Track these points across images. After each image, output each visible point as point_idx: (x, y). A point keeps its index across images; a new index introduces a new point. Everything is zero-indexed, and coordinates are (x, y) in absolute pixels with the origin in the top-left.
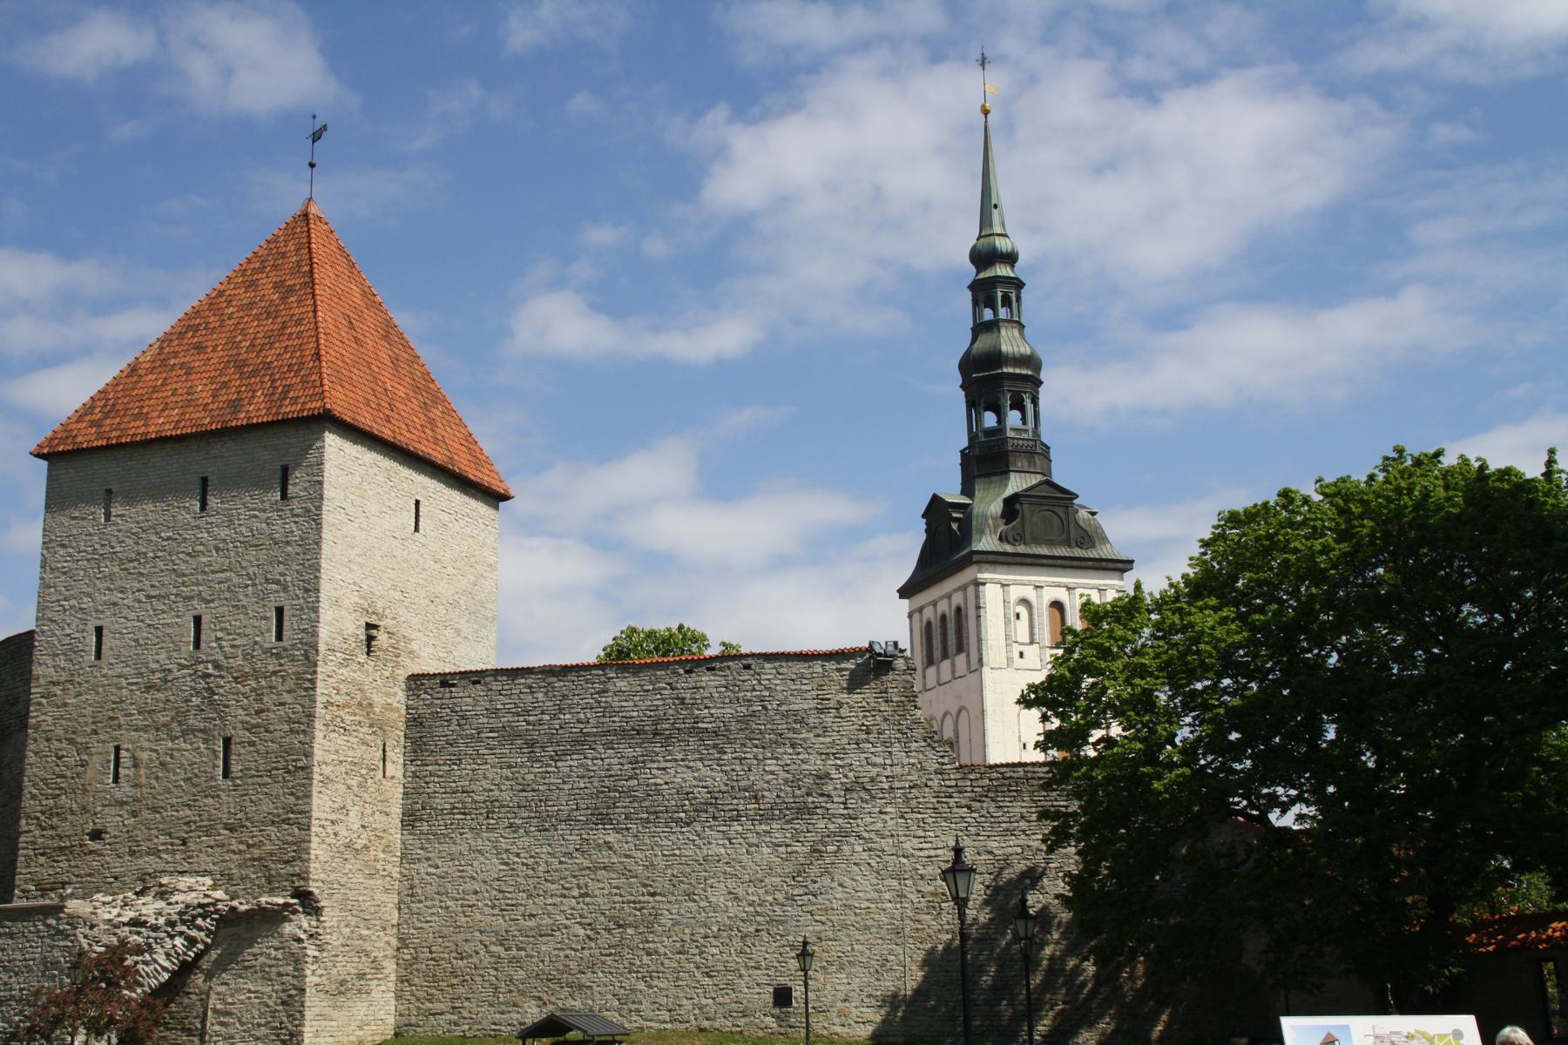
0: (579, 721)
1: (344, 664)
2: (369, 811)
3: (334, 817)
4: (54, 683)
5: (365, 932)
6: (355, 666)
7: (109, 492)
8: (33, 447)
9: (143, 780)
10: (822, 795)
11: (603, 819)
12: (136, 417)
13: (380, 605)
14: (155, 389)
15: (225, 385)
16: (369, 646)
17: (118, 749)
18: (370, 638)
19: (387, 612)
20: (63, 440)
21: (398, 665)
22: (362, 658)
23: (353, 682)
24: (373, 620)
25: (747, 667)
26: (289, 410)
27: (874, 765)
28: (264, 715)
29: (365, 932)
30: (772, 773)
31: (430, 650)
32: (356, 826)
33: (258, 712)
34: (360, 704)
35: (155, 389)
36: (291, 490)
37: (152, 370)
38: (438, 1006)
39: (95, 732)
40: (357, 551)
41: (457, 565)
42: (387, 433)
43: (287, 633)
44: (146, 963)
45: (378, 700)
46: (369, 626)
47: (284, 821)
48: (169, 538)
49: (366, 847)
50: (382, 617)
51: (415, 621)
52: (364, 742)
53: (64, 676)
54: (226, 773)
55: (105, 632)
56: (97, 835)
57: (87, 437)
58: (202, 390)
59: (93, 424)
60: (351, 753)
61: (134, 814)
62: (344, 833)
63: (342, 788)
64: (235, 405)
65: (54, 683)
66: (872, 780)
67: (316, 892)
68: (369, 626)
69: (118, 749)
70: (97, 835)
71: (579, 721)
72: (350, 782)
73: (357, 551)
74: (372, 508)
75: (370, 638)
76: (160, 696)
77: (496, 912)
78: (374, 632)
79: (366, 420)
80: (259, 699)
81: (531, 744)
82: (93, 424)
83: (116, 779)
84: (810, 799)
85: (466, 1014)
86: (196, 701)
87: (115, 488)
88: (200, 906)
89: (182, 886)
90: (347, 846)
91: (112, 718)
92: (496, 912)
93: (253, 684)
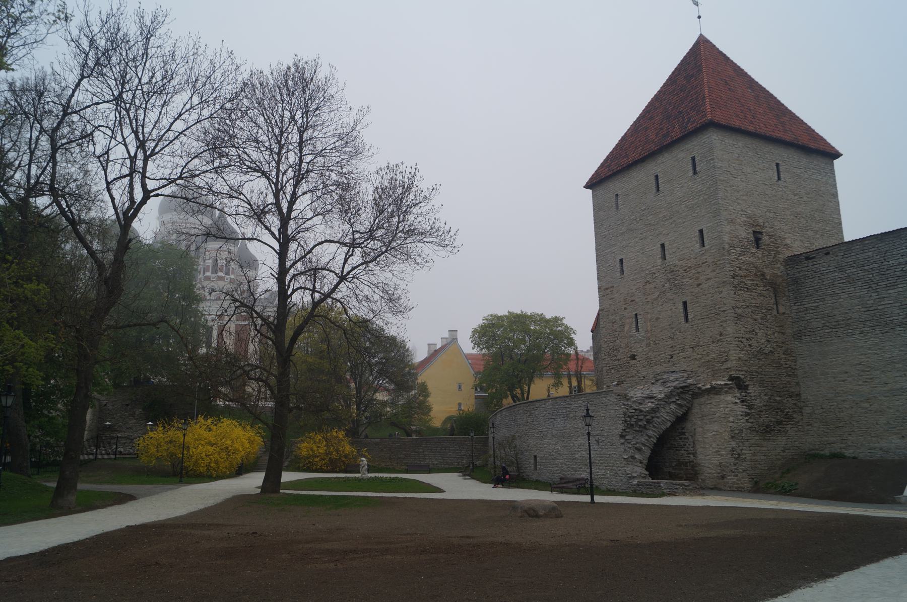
1: (743, 253)
3: (747, 336)
4: (607, 289)
7: (617, 195)
12: (624, 157)
15: (662, 129)
17: (636, 315)
19: (766, 224)
22: (754, 250)
24: (758, 229)
32: (763, 341)
33: (699, 285)
34: (756, 275)
39: (625, 309)
40: (741, 193)
42: (751, 128)
43: (706, 242)
44: (658, 417)
53: (610, 285)
54: (687, 320)
56: (633, 357)
60: (753, 301)
62: (755, 344)
65: (607, 289)
69: (636, 315)
70: (633, 357)
72: (755, 317)
73: (741, 193)
76: (652, 286)
78: (760, 236)
79: (736, 123)
80: (697, 279)
83: (637, 330)
86: (667, 285)
88: (681, 387)
90: (758, 352)
93: (693, 271)
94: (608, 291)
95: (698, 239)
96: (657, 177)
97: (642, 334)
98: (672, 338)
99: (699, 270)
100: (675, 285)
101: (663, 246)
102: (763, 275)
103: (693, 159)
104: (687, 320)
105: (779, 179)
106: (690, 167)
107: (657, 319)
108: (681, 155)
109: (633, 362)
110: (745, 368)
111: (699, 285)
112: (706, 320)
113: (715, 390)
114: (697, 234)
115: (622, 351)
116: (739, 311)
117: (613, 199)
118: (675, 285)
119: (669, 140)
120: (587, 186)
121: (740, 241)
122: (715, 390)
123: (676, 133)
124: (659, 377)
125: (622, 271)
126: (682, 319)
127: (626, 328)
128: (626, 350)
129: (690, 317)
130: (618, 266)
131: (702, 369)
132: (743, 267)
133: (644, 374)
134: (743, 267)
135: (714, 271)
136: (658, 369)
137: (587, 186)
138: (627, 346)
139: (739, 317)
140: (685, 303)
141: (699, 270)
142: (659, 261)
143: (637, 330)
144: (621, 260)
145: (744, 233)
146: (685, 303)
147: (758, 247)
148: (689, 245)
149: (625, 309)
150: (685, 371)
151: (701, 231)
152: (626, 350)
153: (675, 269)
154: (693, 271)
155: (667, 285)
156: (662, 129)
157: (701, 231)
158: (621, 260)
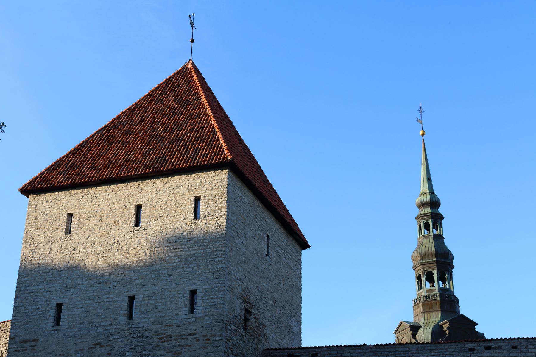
6: (240, 337)
12: (93, 167)
13: (251, 298)
15: (152, 149)
16: (245, 326)
18: (246, 320)
21: (259, 342)
22: (243, 332)
31: (273, 335)
43: (198, 308)
55: (64, 307)
68: (247, 311)
73: (241, 258)
74: (249, 233)
75: (246, 320)
87: (75, 213)
93: (174, 342)
94: (26, 345)
95: (187, 301)
96: (139, 208)
99: (183, 342)
103: (197, 200)
114: (188, 294)
117: (64, 218)
125: (58, 322)
130: (53, 313)
135: (204, 348)
141: (183, 342)
142: (123, 319)
144: (59, 306)
147: (245, 329)
148: (174, 306)
151: (193, 293)
153: (146, 334)
154: (174, 342)
156: (152, 149)
157: (193, 293)
158: (59, 306)
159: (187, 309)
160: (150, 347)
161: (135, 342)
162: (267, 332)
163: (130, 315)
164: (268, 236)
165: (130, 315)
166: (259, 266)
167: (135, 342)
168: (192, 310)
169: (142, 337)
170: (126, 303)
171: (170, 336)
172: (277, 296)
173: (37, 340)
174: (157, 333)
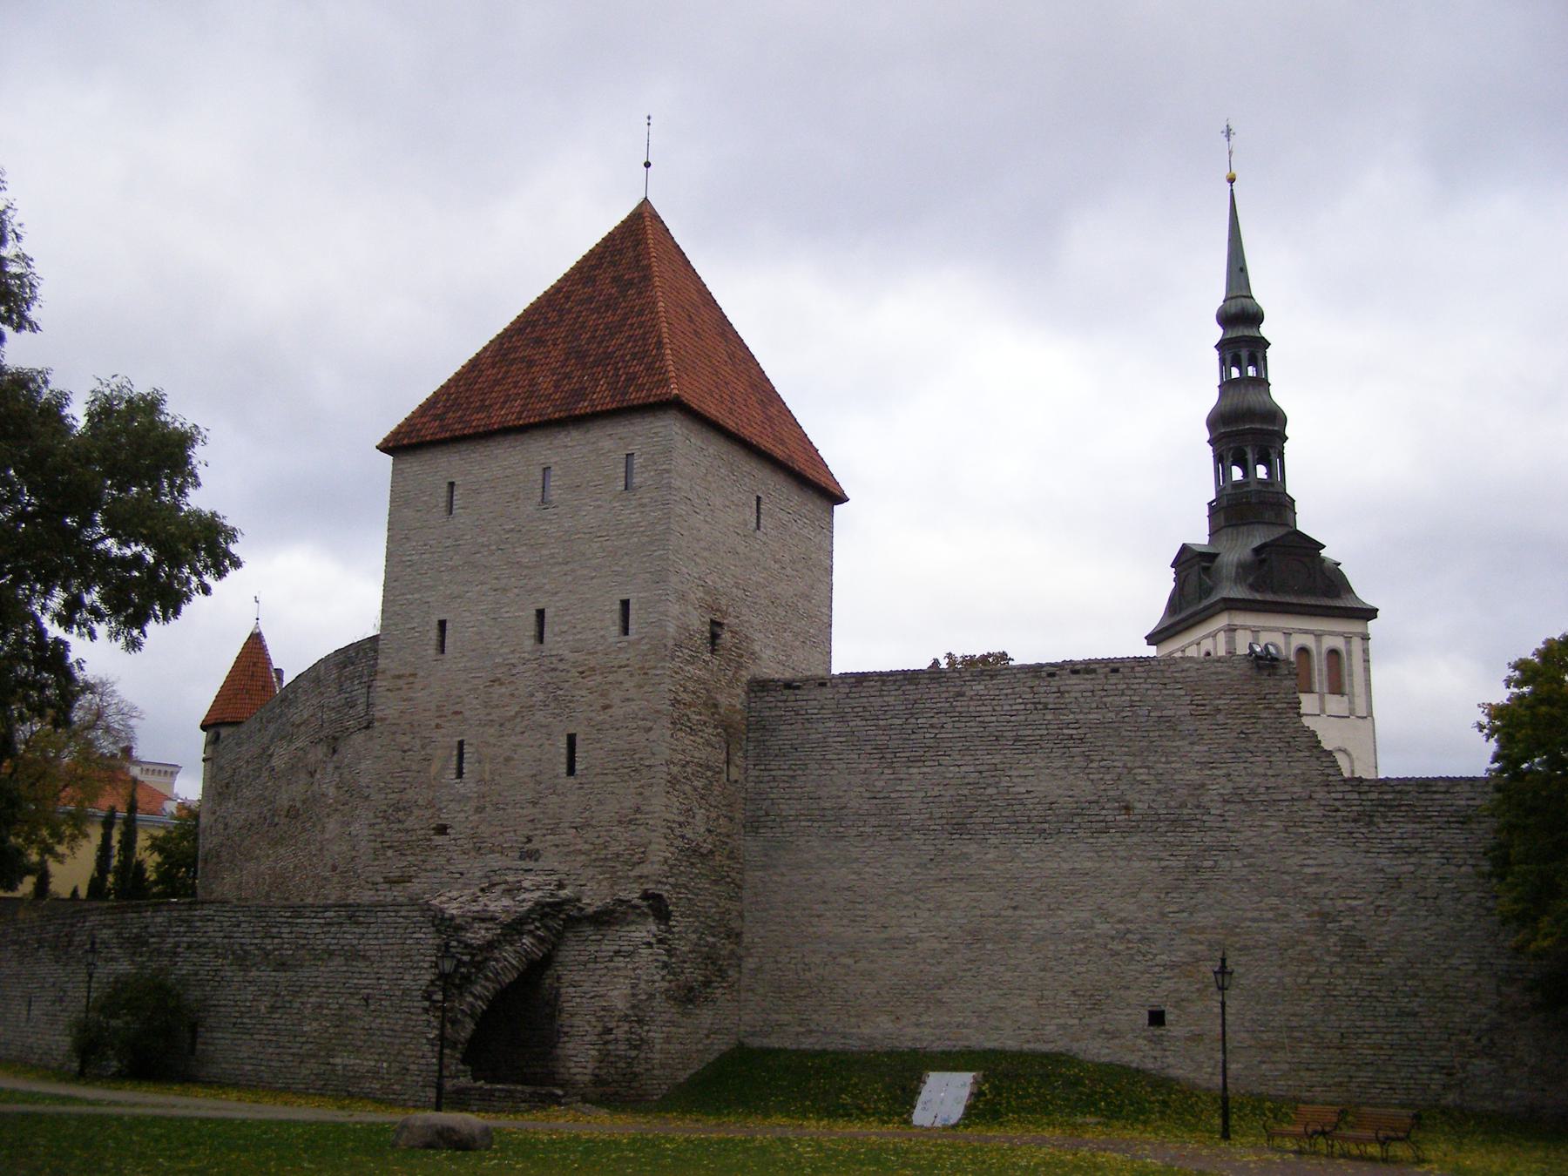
0: (932, 726)
2: (714, 815)
5: (711, 939)
6: (701, 664)
8: (379, 441)
9: (487, 776)
10: (1198, 807)
11: (959, 828)
12: (482, 408)
13: (723, 602)
14: (497, 382)
16: (713, 644)
17: (461, 743)
20: (408, 434)
22: (707, 657)
23: (699, 681)
25: (1115, 671)
26: (634, 397)
27: (1256, 775)
28: (610, 711)
29: (711, 939)
30: (1143, 783)
33: (606, 707)
34: (705, 704)
35: (497, 382)
36: (637, 480)
37: (493, 365)
38: (785, 1018)
39: (438, 726)
40: (703, 544)
41: (799, 566)
42: (731, 424)
43: (632, 627)
45: (723, 700)
46: (713, 622)
47: (630, 821)
48: (512, 530)
49: (711, 852)
50: (725, 614)
51: (756, 621)
52: (708, 743)
54: (571, 770)
55: (448, 625)
56: (442, 830)
57: (430, 431)
58: (545, 383)
59: (435, 417)
61: (480, 810)
63: (687, 788)
64: (580, 394)
65: (399, 677)
66: (1252, 791)
67: (665, 895)
68: (713, 622)
69: (461, 743)
70: (442, 830)
71: (932, 726)
73: (703, 544)
77: (845, 922)
79: (712, 410)
80: (603, 695)
81: (881, 750)
82: (435, 417)
83: (460, 774)
84: (1185, 811)
85: (813, 1026)
86: (540, 696)
89: (526, 884)
91: (456, 713)
92: (845, 922)
93: (599, 678)
95: (617, 616)
97: (468, 786)
98: (535, 804)
99: (611, 678)
100: (556, 699)
101: (541, 614)
102: (716, 706)
104: (571, 770)
105: (758, 528)
106: (621, 470)
107: (508, 759)
108: (607, 444)
109: (439, 840)
110: (672, 880)
111: (606, 707)
112: (611, 778)
113: (604, 919)
114: (617, 607)
115: (416, 812)
116: (675, 770)
118: (556, 699)
119: (584, 407)
120: (385, 447)
121: (691, 637)
122: (604, 919)
123: (601, 397)
124: (496, 879)
126: (563, 769)
127: (434, 769)
128: (428, 813)
129: (578, 767)
130: (434, 634)
131: (590, 872)
132: (690, 686)
133: (461, 868)
134: (690, 686)
136: (495, 861)
137: (385, 447)
138: (430, 804)
139: (673, 781)
140: (571, 740)
141: (611, 678)
142: (529, 643)
143: (460, 774)
144: (442, 624)
145: (698, 622)
146: (571, 740)
147: (713, 651)
148: (598, 625)
149: (438, 726)
150: (553, 872)
151: (625, 604)
152: (428, 813)
153: (561, 666)
155: (540, 696)
157: (625, 604)
158: (442, 624)
159: (615, 629)
160: (566, 685)
161: (547, 678)
162: (757, 648)
163: (540, 637)
164: (759, 498)
165: (540, 637)
166: (741, 549)
167: (547, 678)
168: (625, 631)
169: (554, 670)
170: (533, 619)
171: (593, 669)
172: (778, 590)
173: (414, 675)
174: (575, 664)
